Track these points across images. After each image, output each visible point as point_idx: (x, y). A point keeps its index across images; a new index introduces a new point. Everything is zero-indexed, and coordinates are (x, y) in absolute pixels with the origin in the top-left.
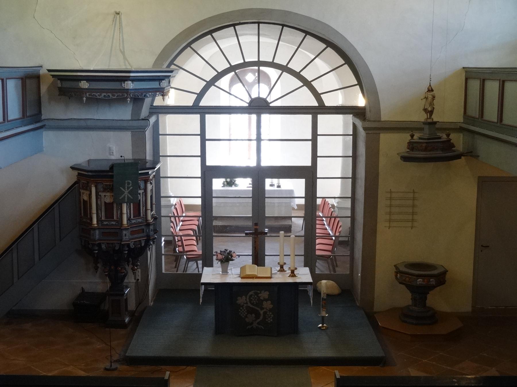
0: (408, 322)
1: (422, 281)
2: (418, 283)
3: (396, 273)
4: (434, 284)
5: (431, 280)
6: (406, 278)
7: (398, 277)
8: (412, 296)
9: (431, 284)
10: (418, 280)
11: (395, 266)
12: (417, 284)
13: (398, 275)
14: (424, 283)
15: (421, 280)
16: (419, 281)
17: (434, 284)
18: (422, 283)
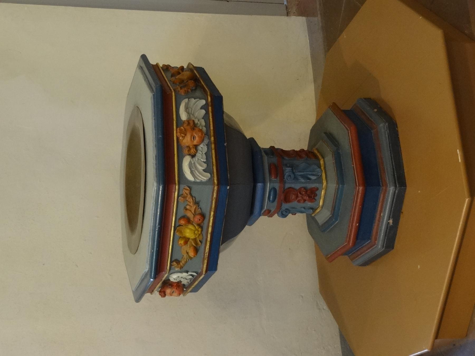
0: (391, 221)
1: (193, 156)
2: (205, 177)
3: (168, 291)
4: (203, 102)
5: (184, 117)
6: (187, 241)
7: (184, 282)
8: (269, 213)
9: (206, 117)
10: (190, 177)
11: (138, 299)
12: (211, 180)
13: (174, 277)
14: (203, 148)
15: (186, 161)
16: (192, 172)
17: (203, 102)
18: (201, 156)
